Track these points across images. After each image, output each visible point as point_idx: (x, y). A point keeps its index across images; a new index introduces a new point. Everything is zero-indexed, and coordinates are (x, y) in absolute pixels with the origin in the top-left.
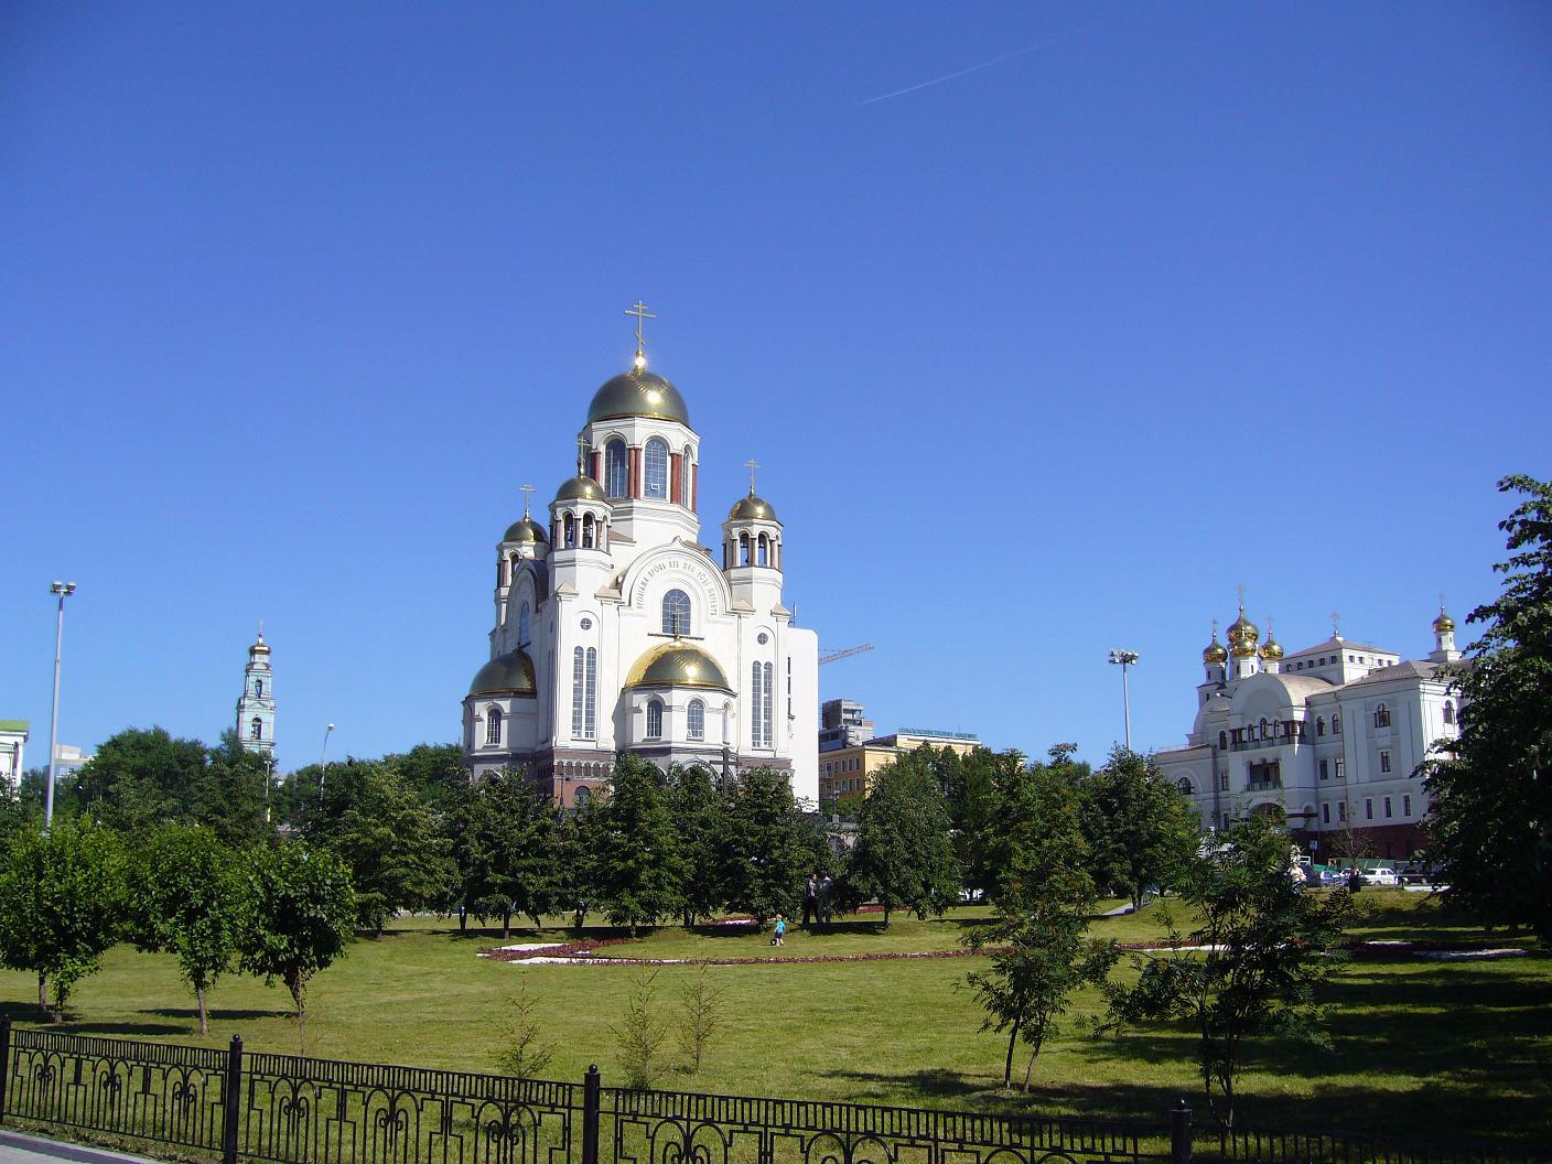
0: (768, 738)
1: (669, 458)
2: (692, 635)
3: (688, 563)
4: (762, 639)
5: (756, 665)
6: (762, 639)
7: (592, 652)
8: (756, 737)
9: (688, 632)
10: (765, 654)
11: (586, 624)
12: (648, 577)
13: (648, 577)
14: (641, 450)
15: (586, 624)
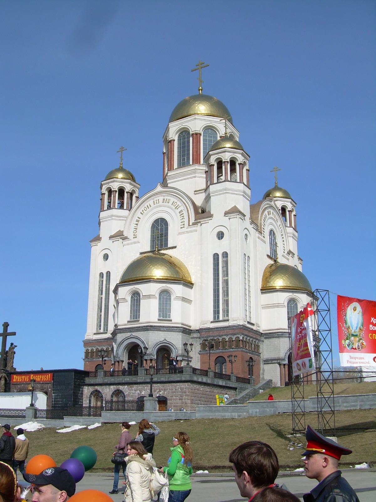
0: (226, 312)
1: (191, 139)
2: (169, 246)
3: (166, 198)
4: (220, 236)
5: (216, 256)
6: (220, 236)
7: (108, 273)
8: (216, 312)
9: (166, 244)
10: (220, 247)
11: (106, 257)
12: (140, 216)
13: (140, 216)
14: (174, 140)
15: (106, 257)
